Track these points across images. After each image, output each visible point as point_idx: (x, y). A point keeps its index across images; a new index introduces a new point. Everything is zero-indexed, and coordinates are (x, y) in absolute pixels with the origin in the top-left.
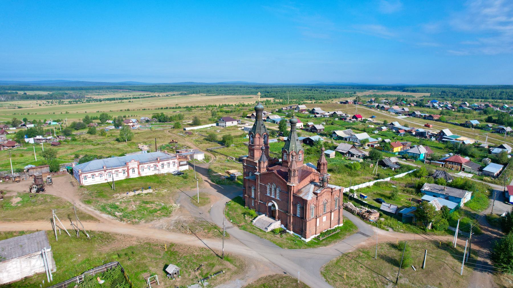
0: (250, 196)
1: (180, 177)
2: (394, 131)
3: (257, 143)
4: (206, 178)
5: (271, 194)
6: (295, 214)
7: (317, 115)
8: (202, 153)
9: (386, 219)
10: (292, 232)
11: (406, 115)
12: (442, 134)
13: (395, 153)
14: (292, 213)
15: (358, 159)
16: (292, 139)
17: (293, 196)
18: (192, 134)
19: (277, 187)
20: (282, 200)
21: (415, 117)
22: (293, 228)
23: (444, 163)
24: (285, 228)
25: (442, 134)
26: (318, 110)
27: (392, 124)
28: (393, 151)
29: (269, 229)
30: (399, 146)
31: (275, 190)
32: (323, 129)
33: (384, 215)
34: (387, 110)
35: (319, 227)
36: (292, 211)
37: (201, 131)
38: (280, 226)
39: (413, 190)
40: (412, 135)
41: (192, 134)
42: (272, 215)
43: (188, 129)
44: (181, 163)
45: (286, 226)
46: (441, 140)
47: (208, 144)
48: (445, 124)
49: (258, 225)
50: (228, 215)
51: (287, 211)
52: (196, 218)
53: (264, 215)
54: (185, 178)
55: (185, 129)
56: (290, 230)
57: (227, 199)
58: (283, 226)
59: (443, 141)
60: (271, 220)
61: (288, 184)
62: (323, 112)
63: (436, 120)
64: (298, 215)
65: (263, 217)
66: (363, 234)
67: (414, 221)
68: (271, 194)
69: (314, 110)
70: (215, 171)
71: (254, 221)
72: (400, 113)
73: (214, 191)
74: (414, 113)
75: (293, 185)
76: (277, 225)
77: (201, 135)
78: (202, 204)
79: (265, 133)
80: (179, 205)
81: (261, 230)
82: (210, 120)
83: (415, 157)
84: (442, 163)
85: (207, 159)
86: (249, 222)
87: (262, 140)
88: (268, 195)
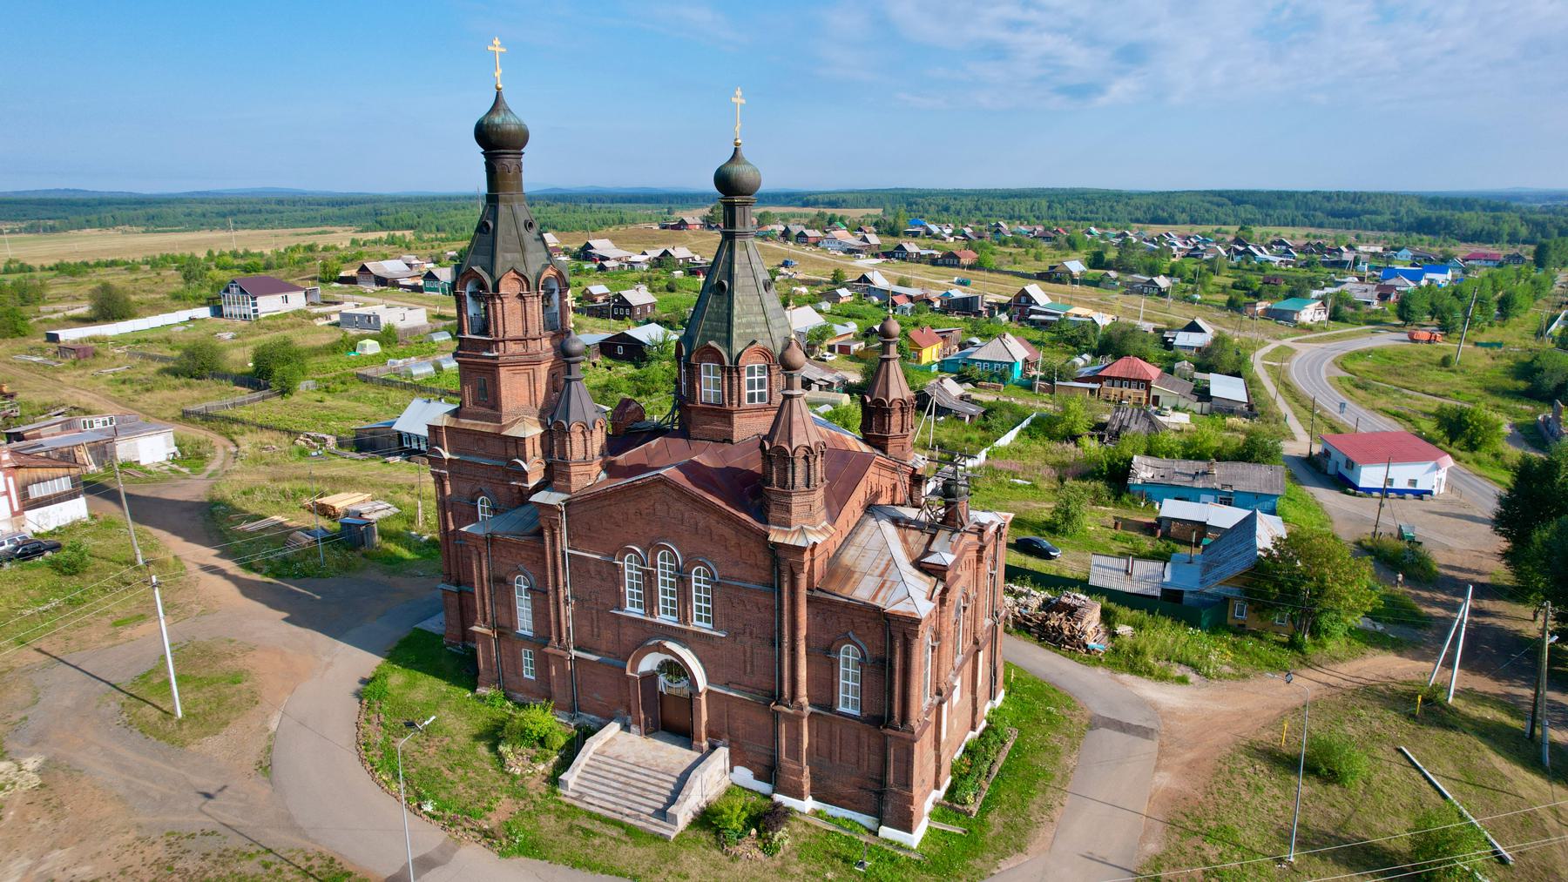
0: (505, 631)
1: (39, 573)
2: (876, 300)
3: (514, 328)
4: (208, 555)
5: (650, 604)
6: (825, 702)
7: (607, 264)
8: (160, 430)
9: (1139, 626)
10: (809, 804)
11: (877, 256)
12: (1023, 300)
13: (929, 366)
14: (803, 699)
15: (826, 395)
16: (739, 282)
17: (810, 601)
18: (95, 354)
19: (690, 560)
20: (734, 635)
21: (904, 259)
22: (814, 777)
23: (1097, 386)
24: (765, 787)
25: (1023, 300)
26: (601, 246)
27: (864, 279)
28: (919, 360)
29: (684, 812)
30: (934, 343)
31: (682, 580)
32: (653, 305)
33: (1124, 612)
34: (816, 245)
35: (948, 741)
36: (803, 690)
37: (139, 339)
38: (726, 782)
39: (1100, 485)
40: (933, 310)
41: (95, 354)
42: (670, 719)
43: (68, 335)
44: (36, 492)
45: (770, 772)
46: (1027, 320)
47: (184, 392)
48: (997, 276)
49: (601, 801)
50: (380, 760)
51: (773, 694)
52: (175, 839)
53: (613, 728)
54: (70, 569)
55: (53, 338)
56: (800, 796)
57: (359, 662)
58: (744, 775)
59: (1033, 322)
60: (675, 756)
61: (776, 536)
62: (621, 253)
63: (970, 267)
64: (848, 701)
65: (618, 746)
66: (1124, 728)
67: (1238, 613)
68: (650, 604)
69: (588, 246)
70: (253, 508)
71: (571, 777)
72: (858, 251)
73: (268, 623)
74: (900, 247)
75: (812, 539)
76: (716, 777)
77: (144, 356)
78: (204, 720)
79: (550, 273)
80: (31, 763)
81: (630, 831)
82: (176, 297)
83: (999, 374)
84: (1090, 385)
85: (191, 455)
86: (536, 786)
87: (535, 307)
88: (633, 611)
